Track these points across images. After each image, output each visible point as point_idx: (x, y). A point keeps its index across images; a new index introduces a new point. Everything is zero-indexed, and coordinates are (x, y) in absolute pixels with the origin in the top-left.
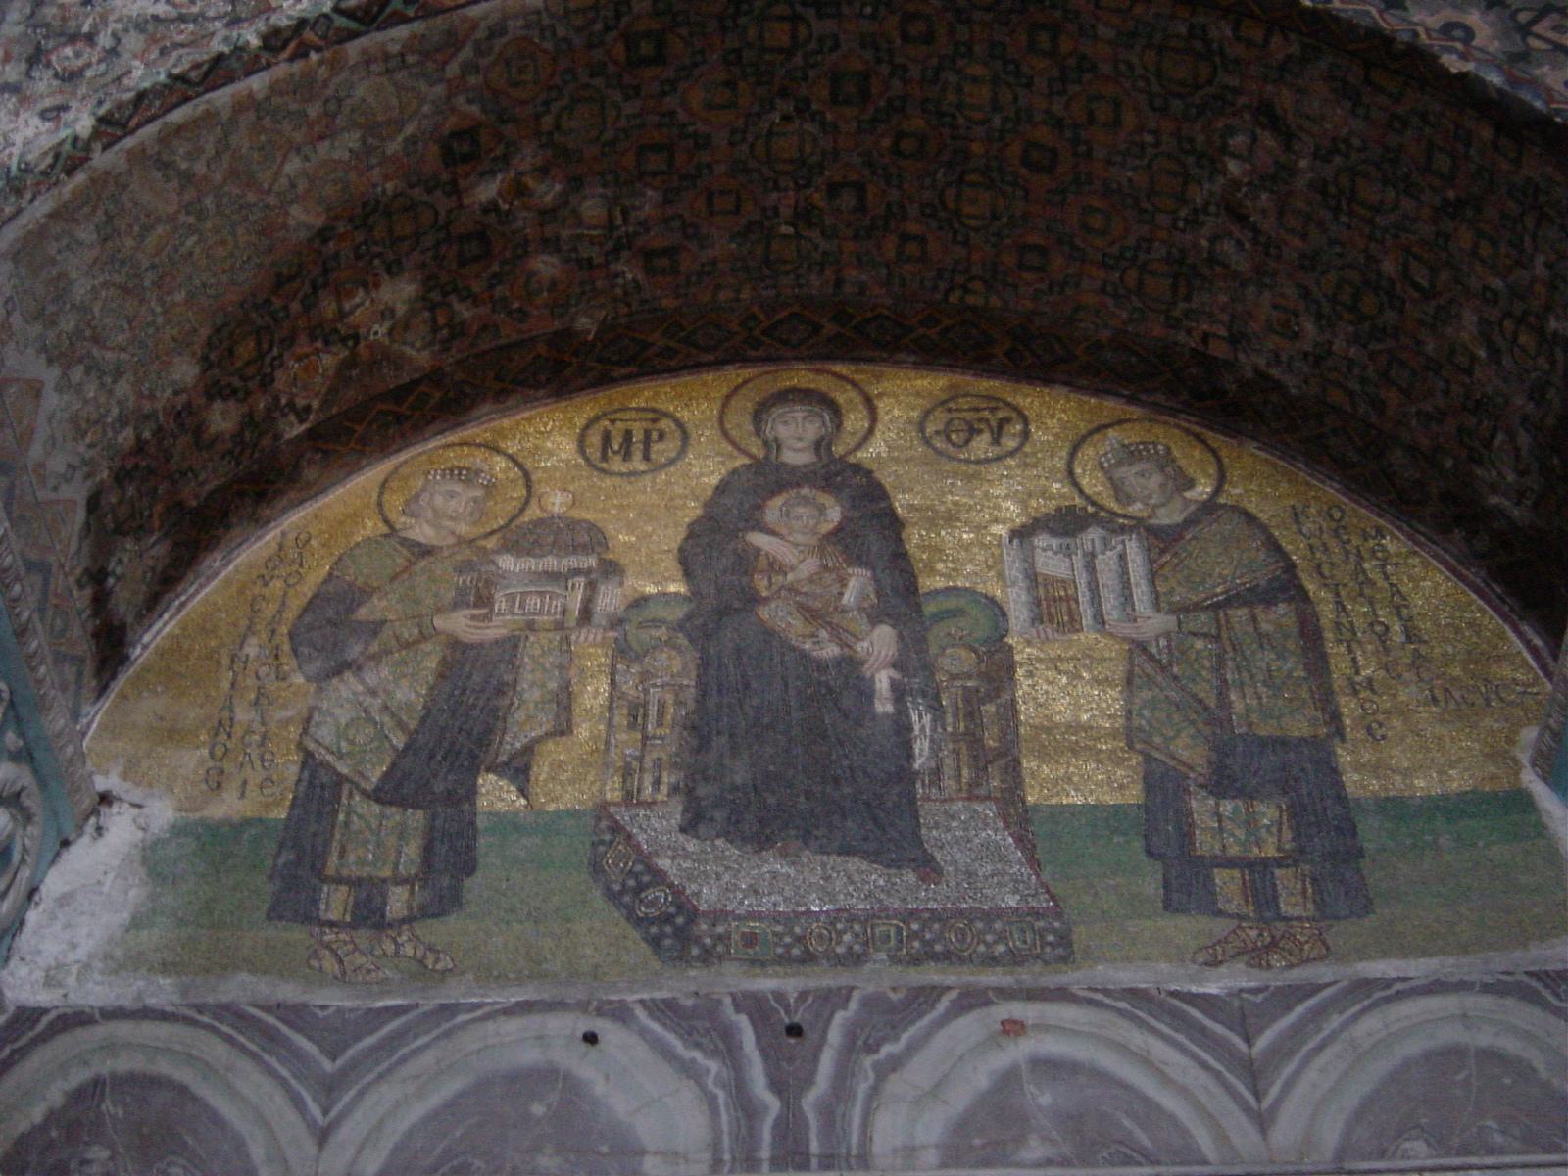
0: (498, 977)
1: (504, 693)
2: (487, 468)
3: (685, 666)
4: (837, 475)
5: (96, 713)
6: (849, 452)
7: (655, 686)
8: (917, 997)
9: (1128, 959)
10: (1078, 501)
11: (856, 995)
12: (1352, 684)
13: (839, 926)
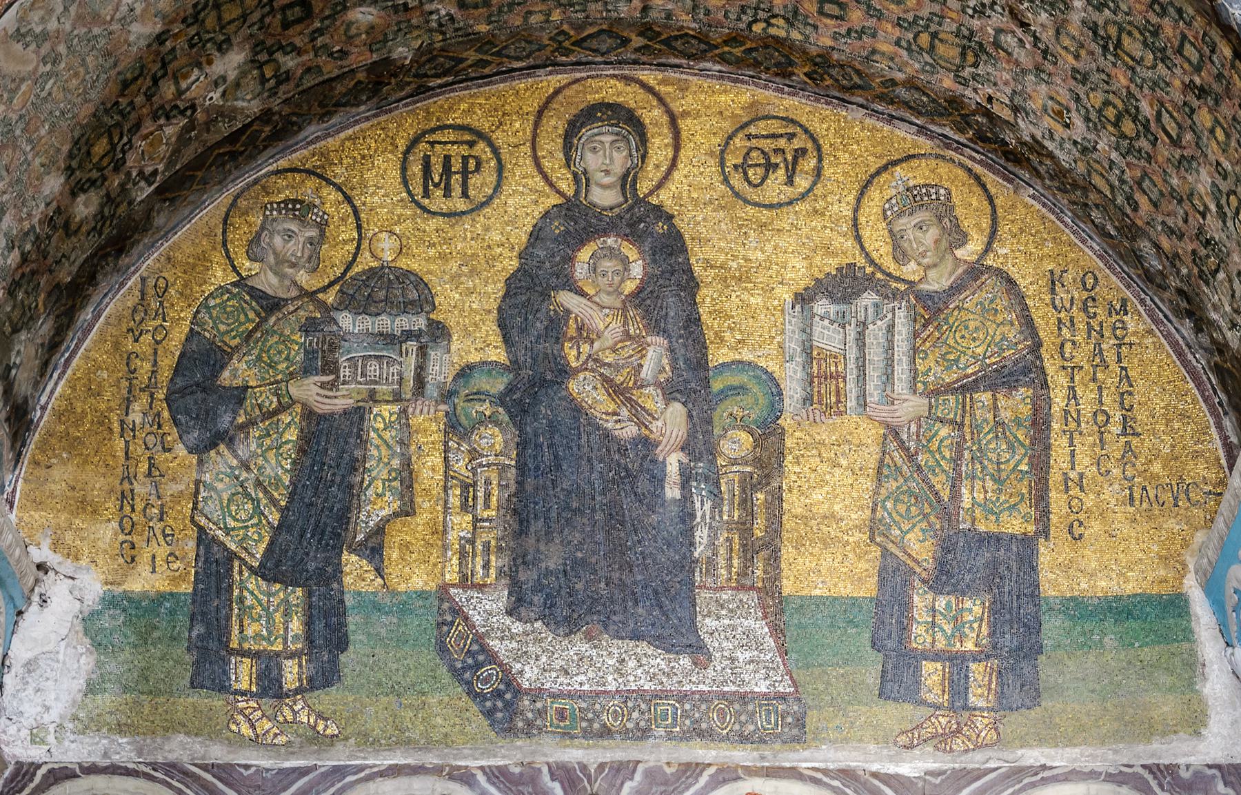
0: (372, 744)
1: (356, 470)
2: (317, 202)
3: (506, 442)
4: (640, 220)
5: (17, 481)
6: (651, 193)
7: (481, 465)
8: (685, 772)
9: (846, 740)
10: (861, 261)
11: (640, 768)
12: (1066, 478)
13: (630, 704)
